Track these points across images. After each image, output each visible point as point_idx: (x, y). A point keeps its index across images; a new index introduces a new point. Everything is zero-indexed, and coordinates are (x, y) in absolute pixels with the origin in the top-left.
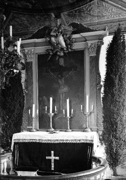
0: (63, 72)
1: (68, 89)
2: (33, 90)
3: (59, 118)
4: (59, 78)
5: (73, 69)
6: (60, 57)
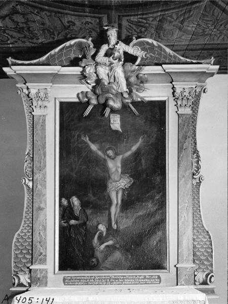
1: (131, 181)
2: (46, 181)
3: (107, 246)
5: (140, 139)
6: (113, 111)
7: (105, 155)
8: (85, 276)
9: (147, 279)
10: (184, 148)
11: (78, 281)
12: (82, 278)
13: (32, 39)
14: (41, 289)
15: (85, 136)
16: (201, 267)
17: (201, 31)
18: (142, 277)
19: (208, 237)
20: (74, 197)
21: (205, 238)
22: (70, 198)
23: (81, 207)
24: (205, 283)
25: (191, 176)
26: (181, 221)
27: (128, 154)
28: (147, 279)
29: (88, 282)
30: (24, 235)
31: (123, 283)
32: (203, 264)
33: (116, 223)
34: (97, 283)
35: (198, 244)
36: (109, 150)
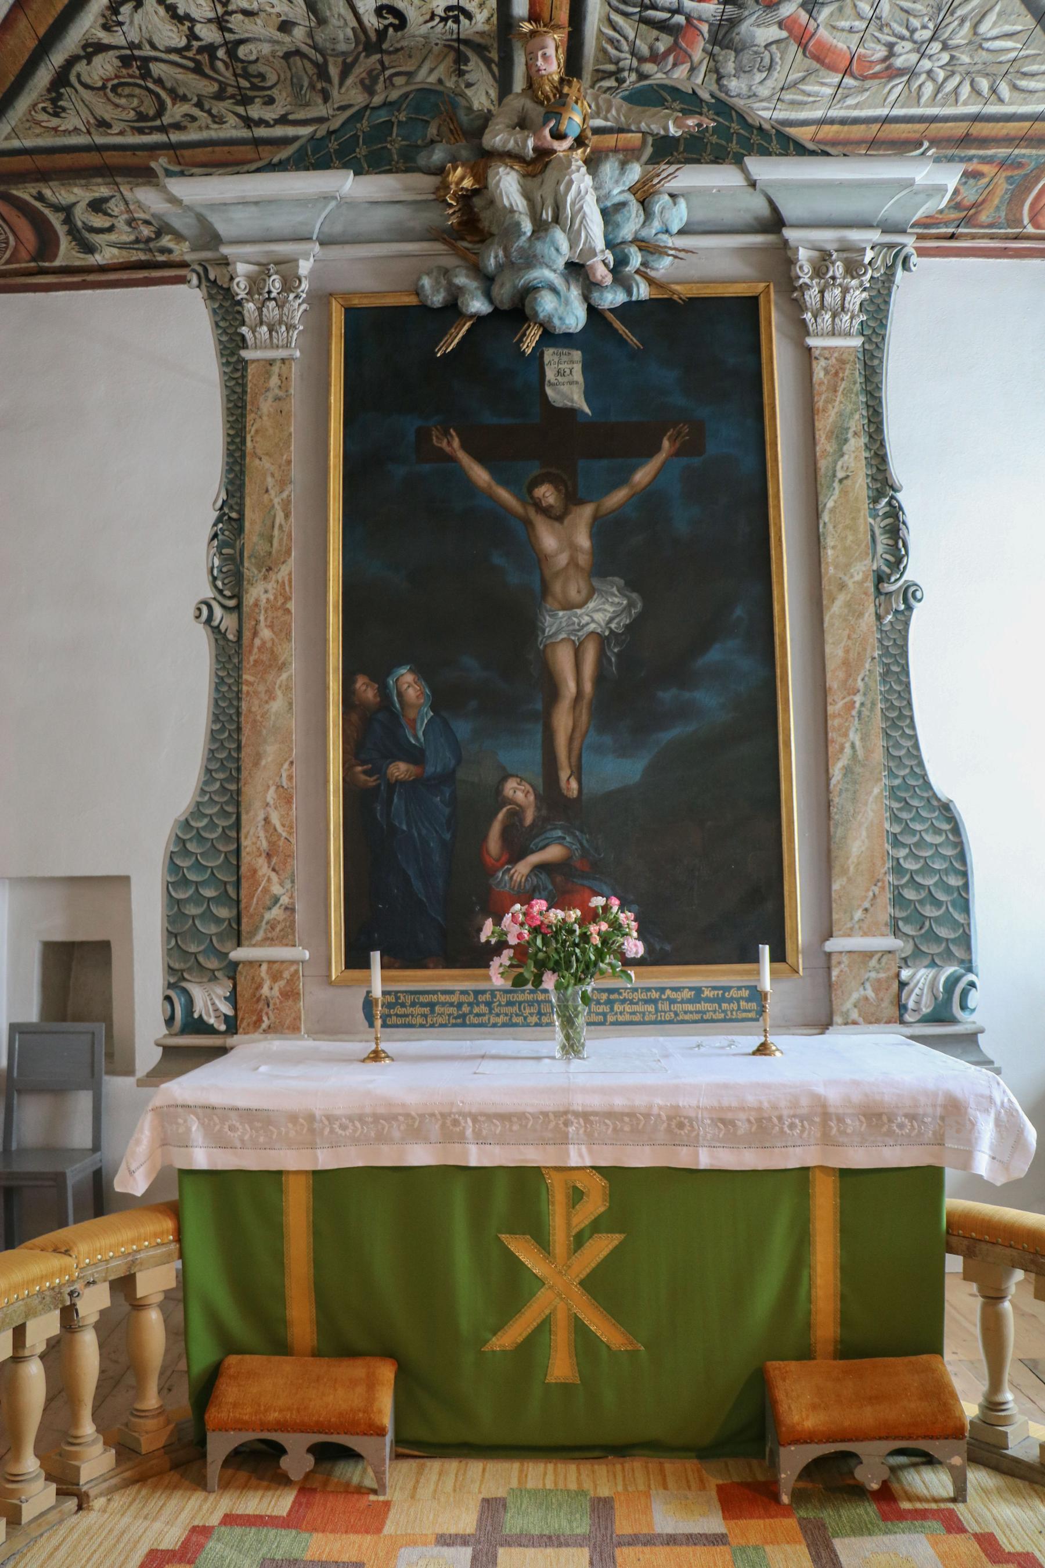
0: (582, 464)
1: (631, 605)
4: (546, 511)
5: (666, 444)
6: (550, 337)
7: (524, 503)
8: (452, 992)
9: (708, 1000)
10: (840, 474)
11: (426, 1010)
12: (442, 998)
13: (246, 101)
14: (276, 1044)
15: (446, 433)
16: (924, 948)
17: (881, 52)
18: (687, 994)
19: (946, 827)
20: (403, 670)
21: (938, 831)
22: (389, 673)
23: (433, 708)
24: (941, 1015)
25: (870, 585)
26: (840, 764)
27: (618, 497)
28: (708, 1000)
29: (464, 1016)
30: (204, 828)
31: (610, 1018)
32: (932, 937)
33: (578, 772)
34: (500, 1020)
35: (912, 855)
36: (542, 483)
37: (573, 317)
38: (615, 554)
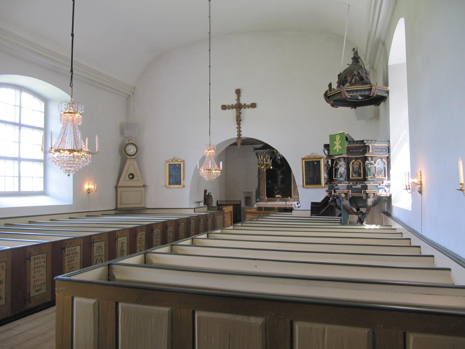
37: (279, 158)
38: (282, 173)
